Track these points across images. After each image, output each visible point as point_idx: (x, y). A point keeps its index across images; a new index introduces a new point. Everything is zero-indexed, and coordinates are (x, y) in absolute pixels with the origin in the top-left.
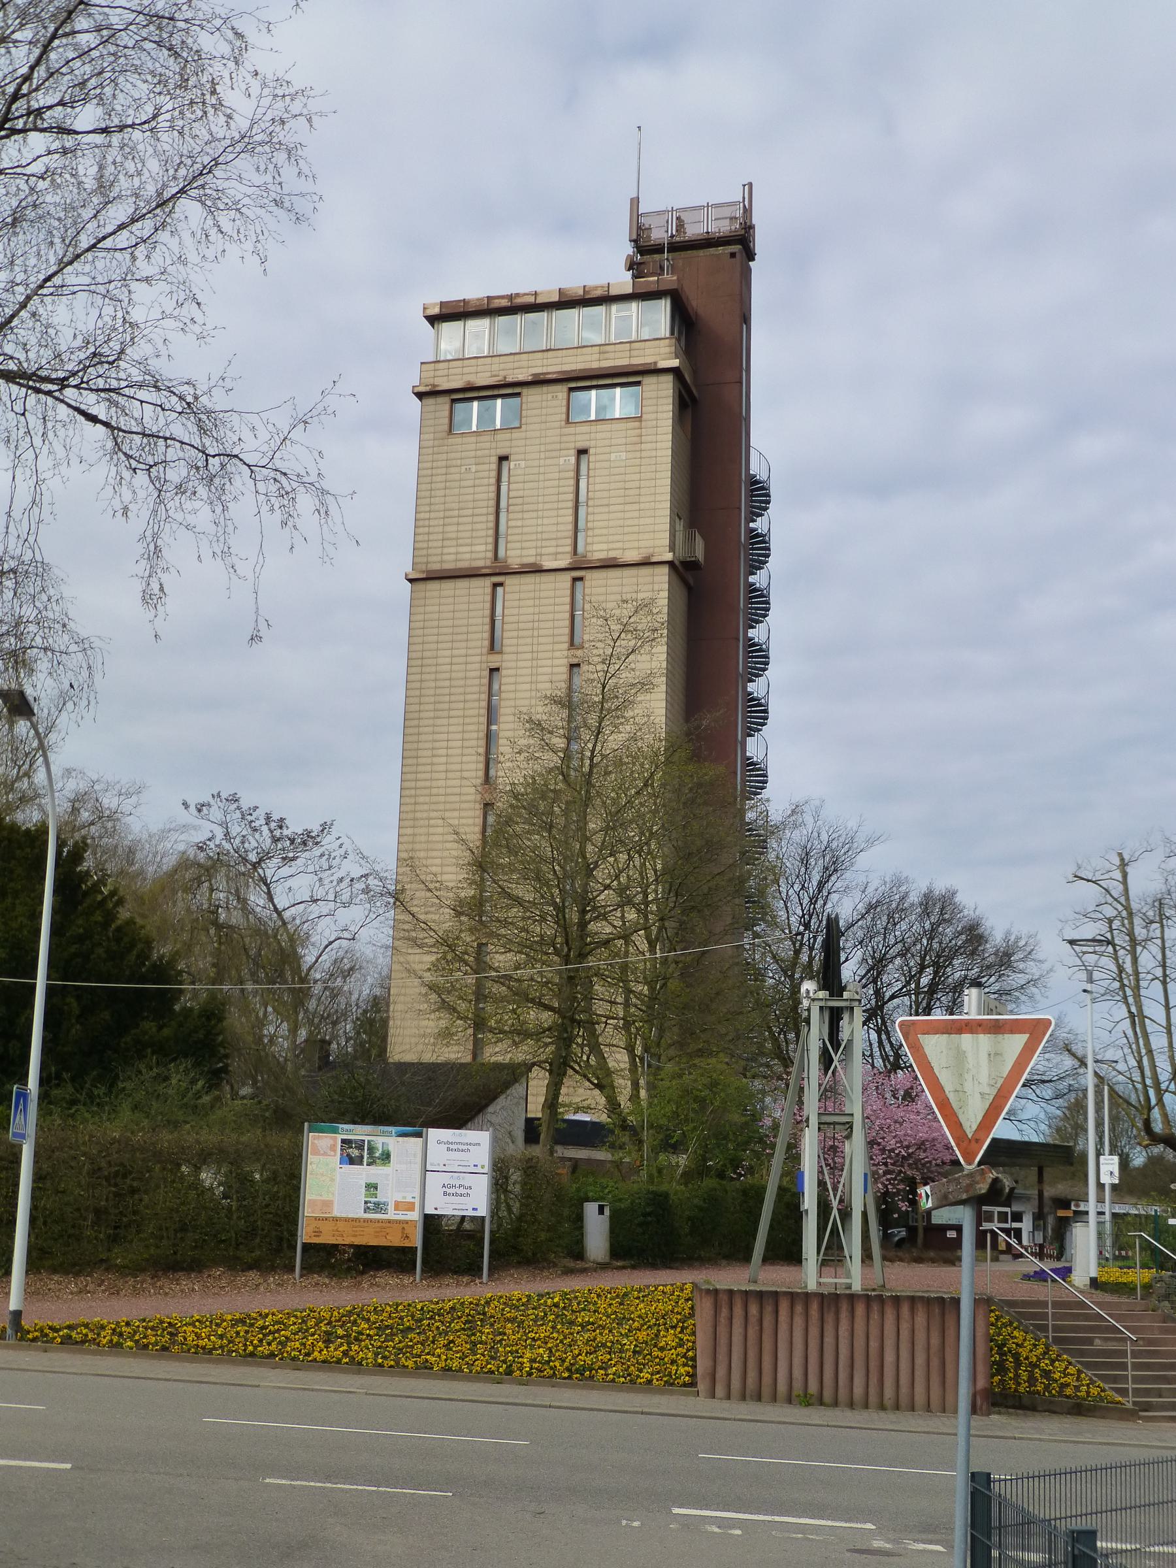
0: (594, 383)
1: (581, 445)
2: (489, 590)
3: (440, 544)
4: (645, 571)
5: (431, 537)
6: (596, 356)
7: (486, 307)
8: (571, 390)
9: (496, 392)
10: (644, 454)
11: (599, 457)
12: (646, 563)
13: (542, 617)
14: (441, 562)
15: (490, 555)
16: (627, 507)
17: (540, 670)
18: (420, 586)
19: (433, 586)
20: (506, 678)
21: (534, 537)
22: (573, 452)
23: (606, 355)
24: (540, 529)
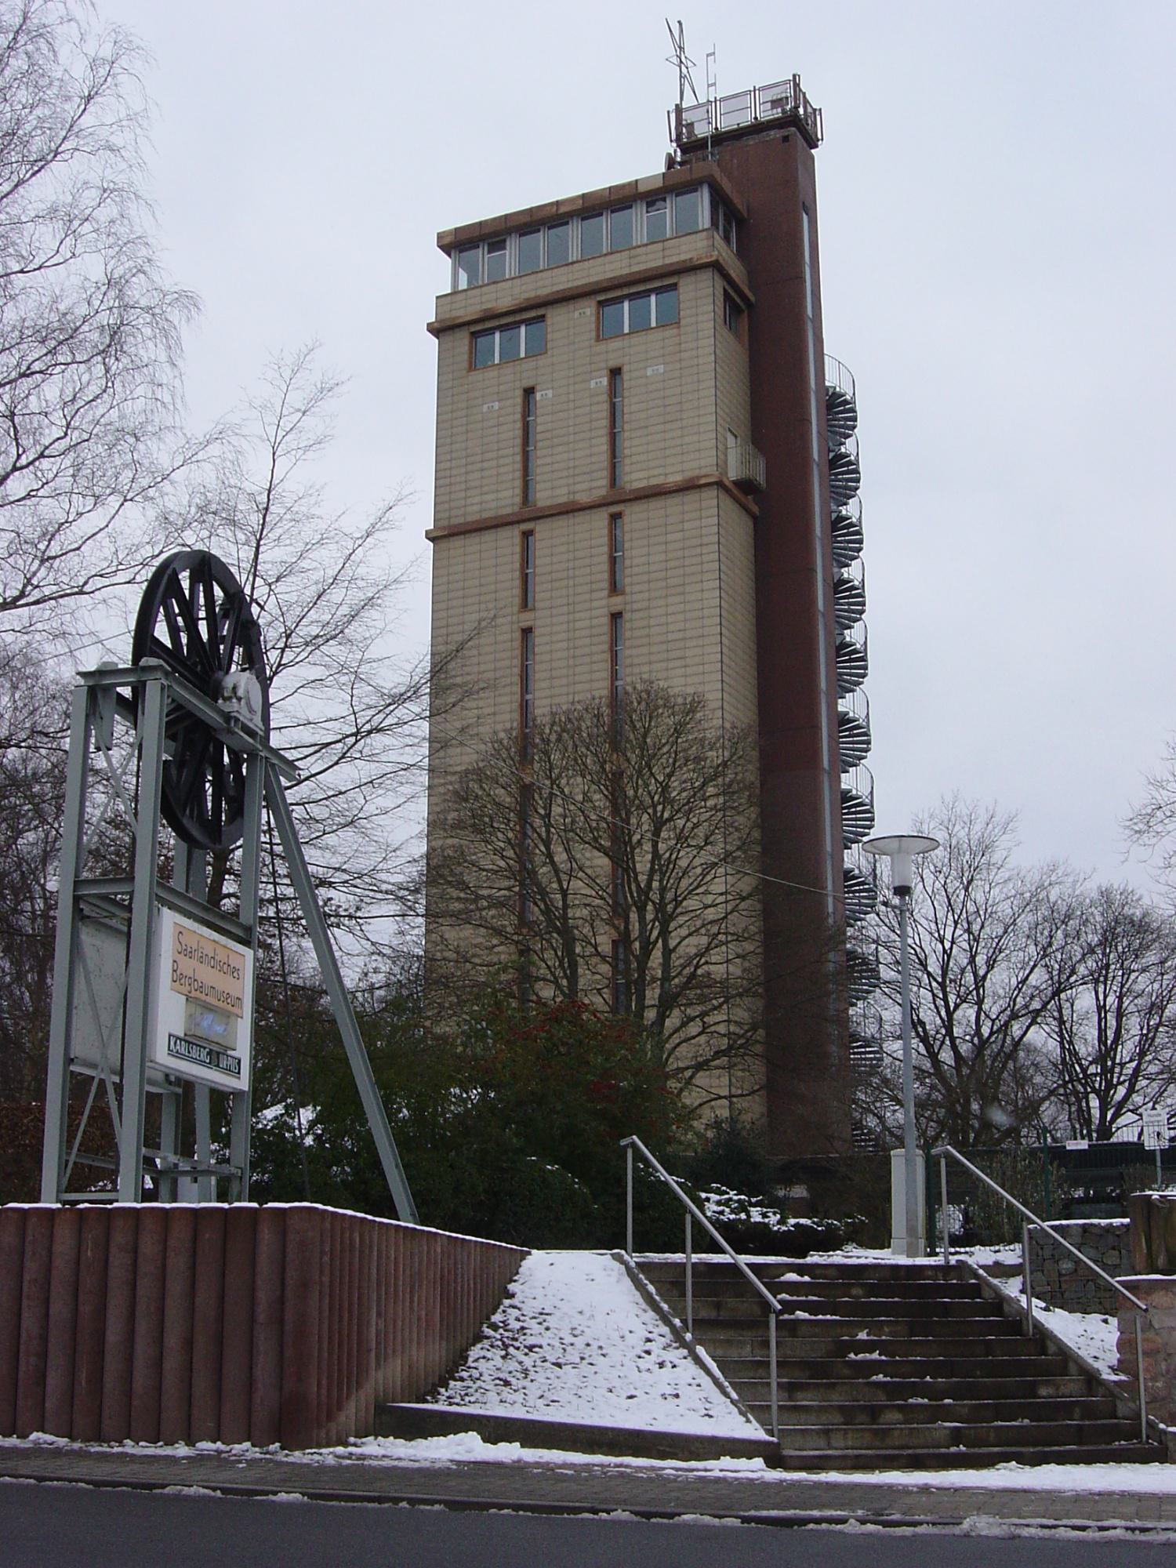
0: (626, 291)
1: (613, 364)
2: (517, 540)
3: (463, 494)
4: (691, 498)
5: (453, 488)
6: (626, 262)
7: (503, 226)
8: (601, 304)
9: (518, 318)
10: (684, 364)
11: (634, 375)
12: (690, 486)
13: (577, 563)
14: (464, 515)
15: (518, 500)
16: (668, 426)
17: (578, 625)
18: (444, 544)
19: (457, 542)
20: (539, 639)
21: (565, 474)
22: (605, 372)
23: (638, 259)
24: (571, 464)
